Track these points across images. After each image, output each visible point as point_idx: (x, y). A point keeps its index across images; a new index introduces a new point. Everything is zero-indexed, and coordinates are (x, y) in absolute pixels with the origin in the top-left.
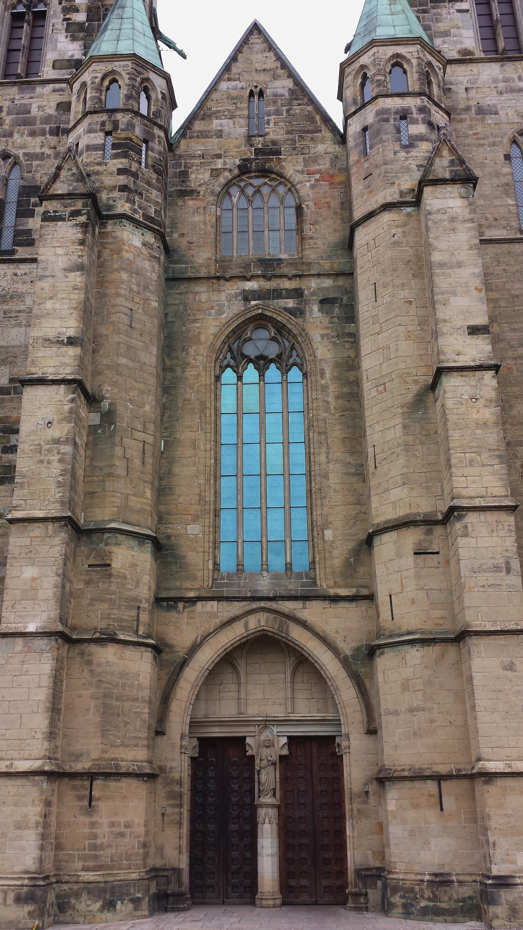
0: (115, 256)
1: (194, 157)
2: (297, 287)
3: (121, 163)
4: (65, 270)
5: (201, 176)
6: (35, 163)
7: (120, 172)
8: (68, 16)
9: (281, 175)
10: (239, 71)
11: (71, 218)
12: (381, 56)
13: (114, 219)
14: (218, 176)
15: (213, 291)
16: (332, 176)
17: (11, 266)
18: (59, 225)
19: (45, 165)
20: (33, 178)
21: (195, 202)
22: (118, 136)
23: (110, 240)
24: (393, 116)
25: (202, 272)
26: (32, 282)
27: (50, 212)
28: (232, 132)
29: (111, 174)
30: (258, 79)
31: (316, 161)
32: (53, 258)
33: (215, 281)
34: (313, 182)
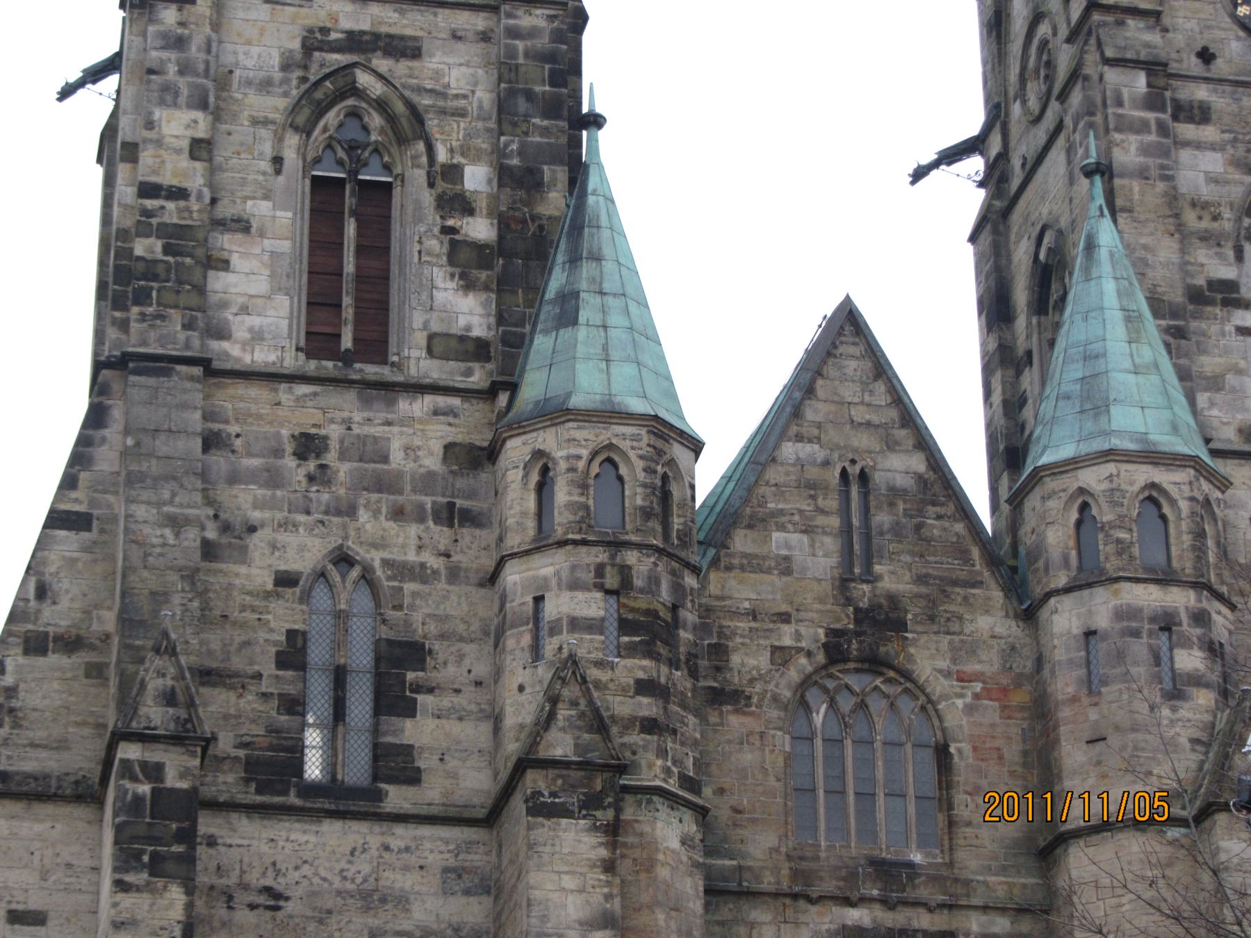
0: (643, 876)
1: (736, 614)
2: (945, 927)
3: (641, 667)
4: (581, 923)
5: (752, 662)
6: (409, 587)
7: (645, 687)
8: (450, 222)
9: (907, 675)
10: (819, 418)
11: (584, 812)
12: (1123, 486)
13: (636, 793)
14: (785, 663)
15: (785, 922)
16: (1005, 690)
17: (377, 829)
18: (563, 826)
19: (430, 594)
20: (407, 623)
21: (743, 719)
22: (632, 604)
23: (630, 839)
24: (1147, 627)
25: (766, 881)
26: (421, 867)
27: (543, 796)
28: (810, 565)
29: (624, 690)
30: (856, 443)
31: (974, 652)
32: (555, 897)
33: (788, 901)
34: (968, 700)
